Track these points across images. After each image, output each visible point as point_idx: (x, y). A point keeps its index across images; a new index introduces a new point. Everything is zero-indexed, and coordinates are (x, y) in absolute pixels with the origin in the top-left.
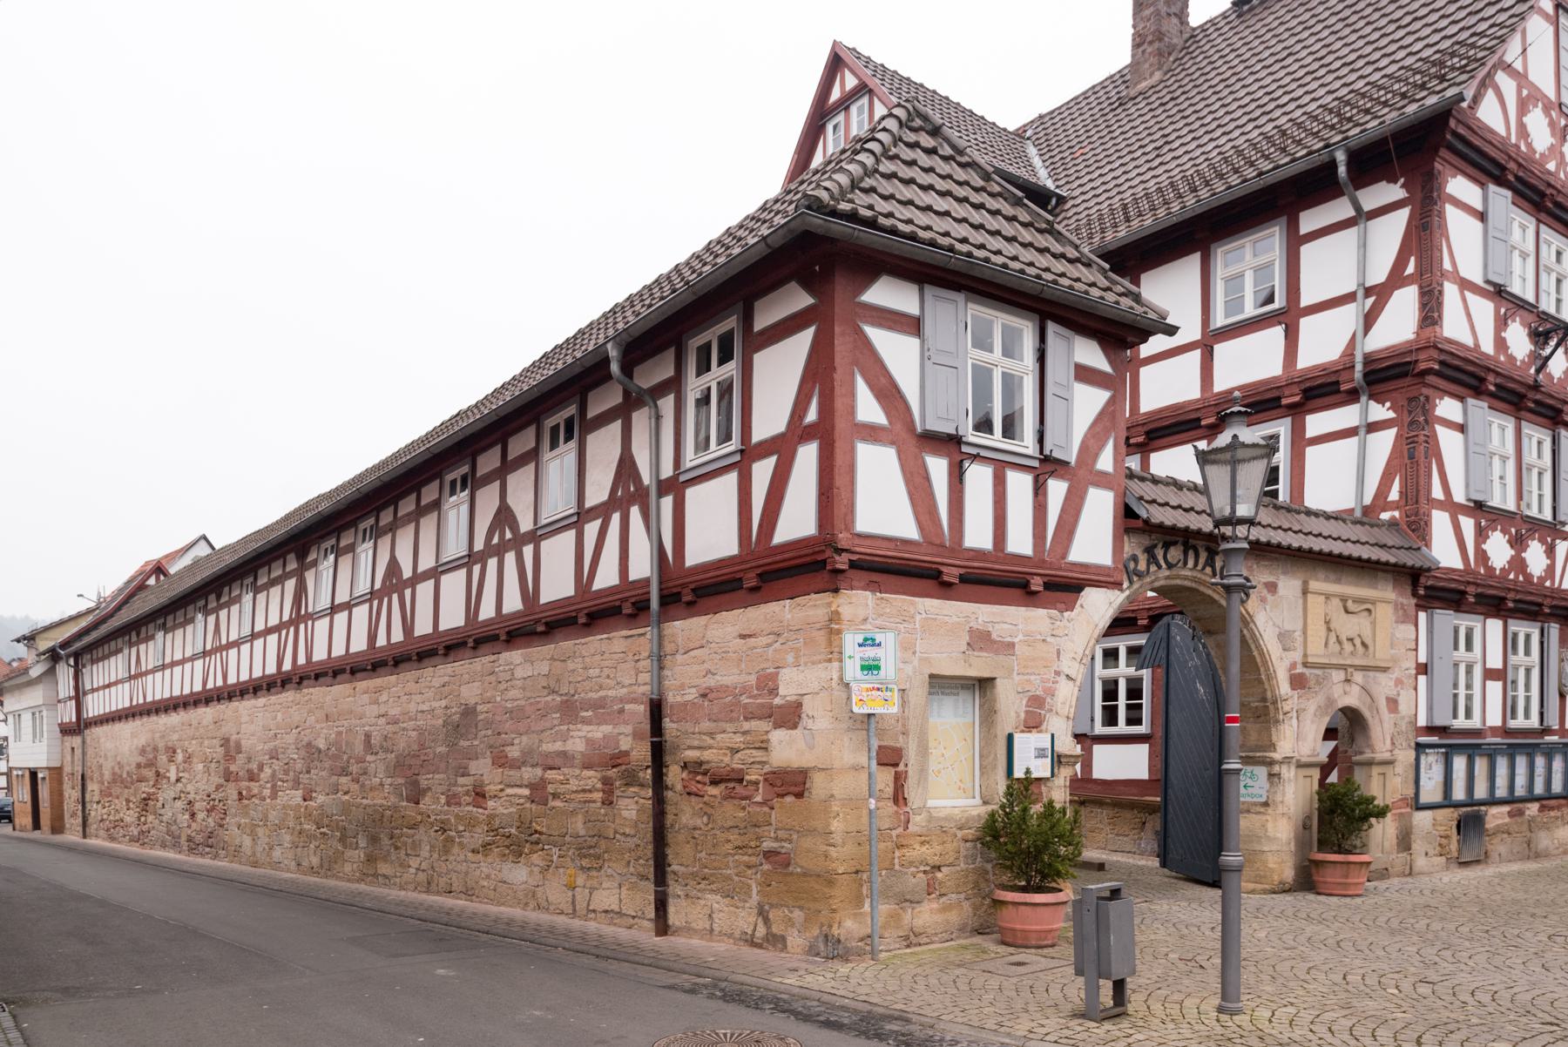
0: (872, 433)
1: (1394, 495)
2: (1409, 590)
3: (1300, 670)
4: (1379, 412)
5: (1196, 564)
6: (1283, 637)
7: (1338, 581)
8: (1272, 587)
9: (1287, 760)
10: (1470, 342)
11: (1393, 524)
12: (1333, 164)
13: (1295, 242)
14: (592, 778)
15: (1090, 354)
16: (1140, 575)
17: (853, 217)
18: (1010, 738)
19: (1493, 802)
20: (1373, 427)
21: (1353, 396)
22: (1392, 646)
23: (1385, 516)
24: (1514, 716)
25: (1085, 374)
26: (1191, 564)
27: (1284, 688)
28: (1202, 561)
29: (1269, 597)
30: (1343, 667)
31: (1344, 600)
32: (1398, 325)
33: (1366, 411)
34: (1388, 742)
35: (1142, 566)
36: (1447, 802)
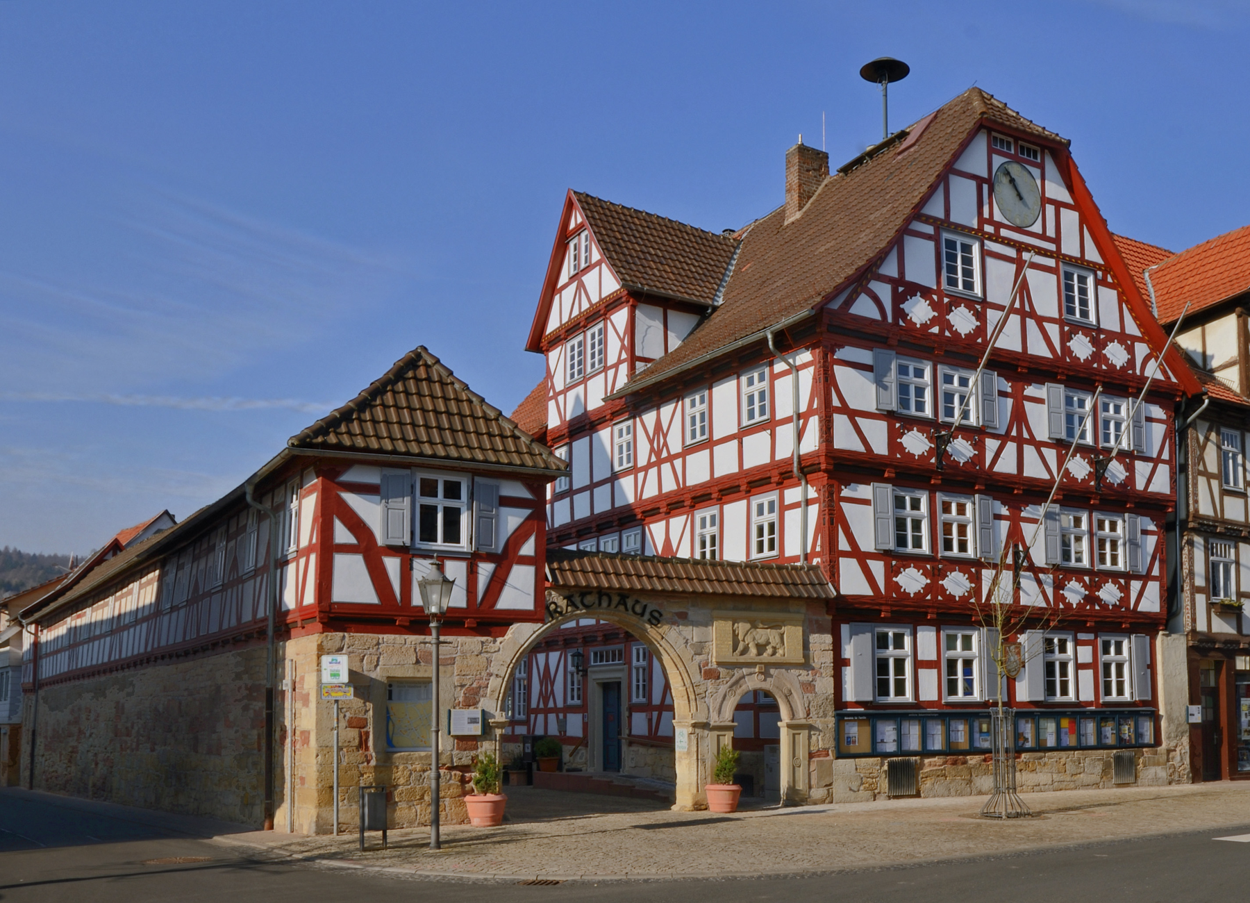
0: (346, 549)
1: (818, 549)
5: (609, 605)
10: (860, 448)
11: (817, 567)
13: (774, 377)
20: (808, 502)
23: (815, 561)
26: (605, 604)
28: (615, 602)
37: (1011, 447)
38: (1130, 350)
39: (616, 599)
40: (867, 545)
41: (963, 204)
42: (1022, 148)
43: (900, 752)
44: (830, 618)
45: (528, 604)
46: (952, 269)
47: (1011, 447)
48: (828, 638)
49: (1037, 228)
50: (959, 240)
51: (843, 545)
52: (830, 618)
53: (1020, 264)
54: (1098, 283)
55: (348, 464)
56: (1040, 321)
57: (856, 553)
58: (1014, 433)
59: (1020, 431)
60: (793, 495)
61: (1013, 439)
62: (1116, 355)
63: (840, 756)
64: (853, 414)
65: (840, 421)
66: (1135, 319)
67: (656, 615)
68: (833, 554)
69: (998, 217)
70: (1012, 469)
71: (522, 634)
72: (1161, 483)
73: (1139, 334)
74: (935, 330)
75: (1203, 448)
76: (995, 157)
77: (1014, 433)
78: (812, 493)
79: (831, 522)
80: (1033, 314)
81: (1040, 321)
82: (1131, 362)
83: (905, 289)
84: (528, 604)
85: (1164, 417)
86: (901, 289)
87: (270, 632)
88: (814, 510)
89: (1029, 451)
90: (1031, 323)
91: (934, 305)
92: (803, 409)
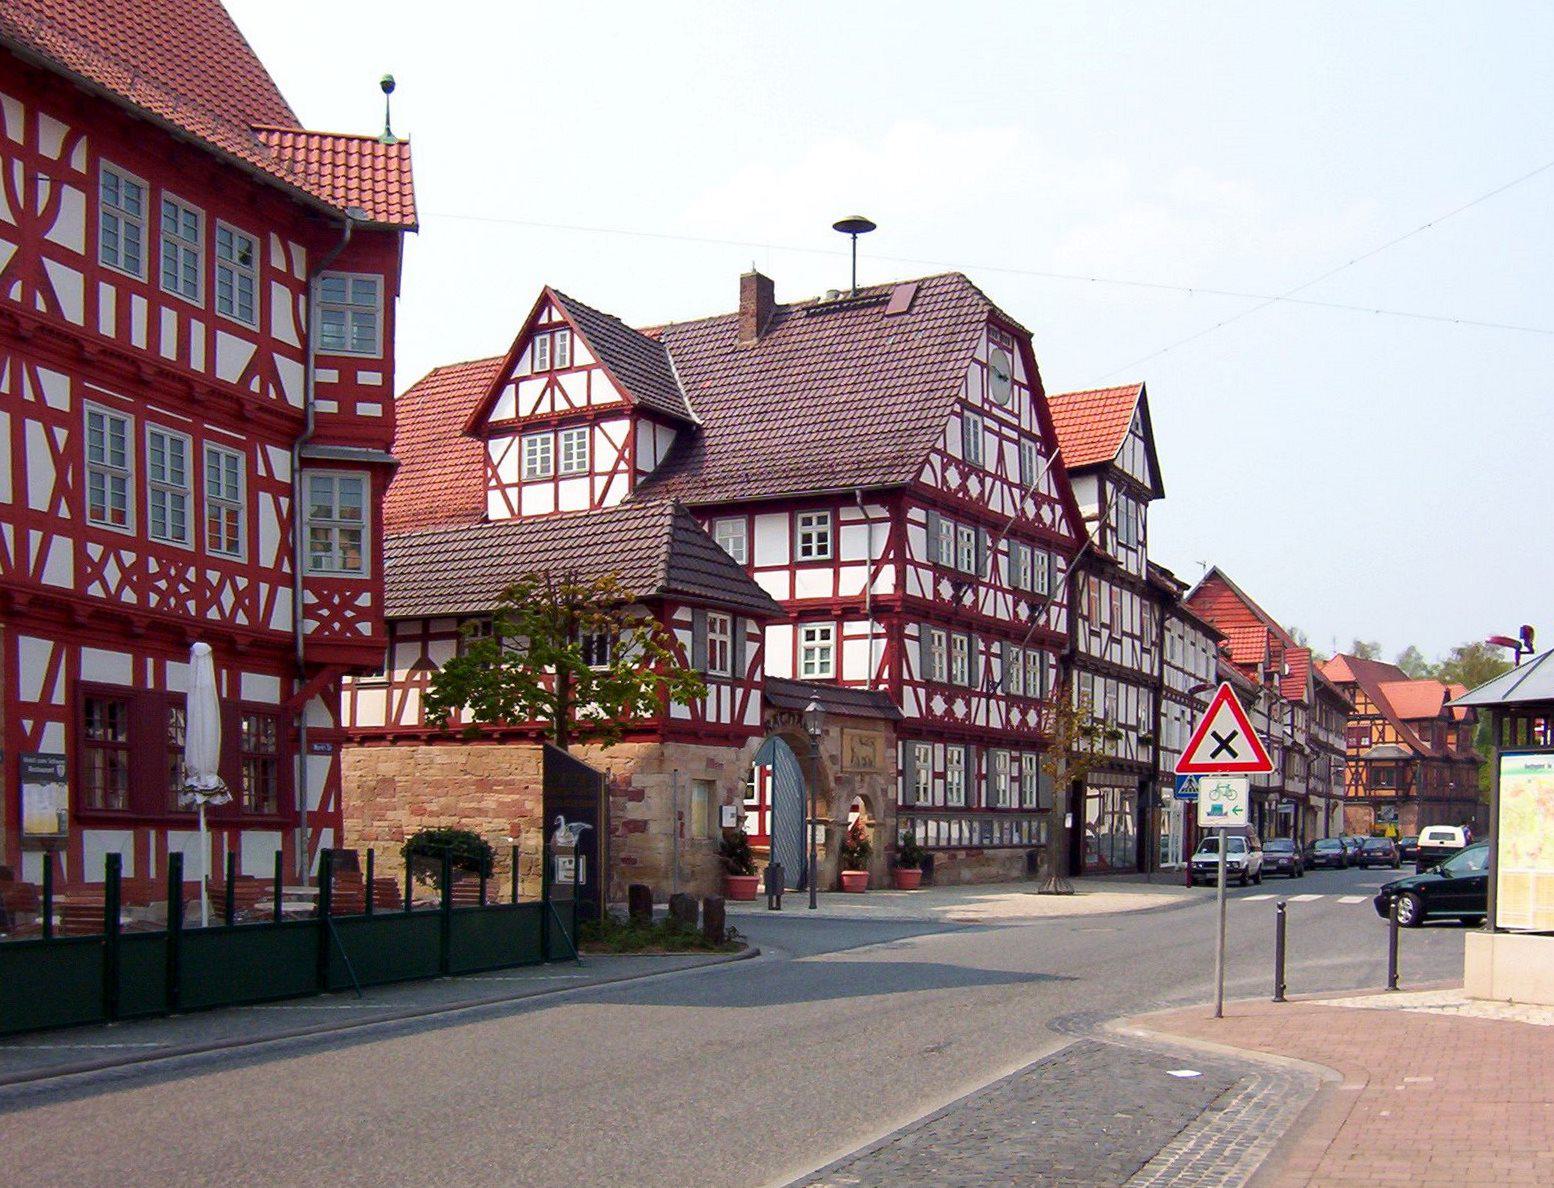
1: (886, 675)
4: (880, 629)
14: (503, 823)
20: (877, 636)
21: (865, 618)
23: (882, 687)
32: (886, 584)
44: (895, 735)
47: (991, 591)
49: (1008, 407)
52: (895, 735)
60: (852, 628)
69: (991, 398)
88: (883, 642)
92: (878, 556)
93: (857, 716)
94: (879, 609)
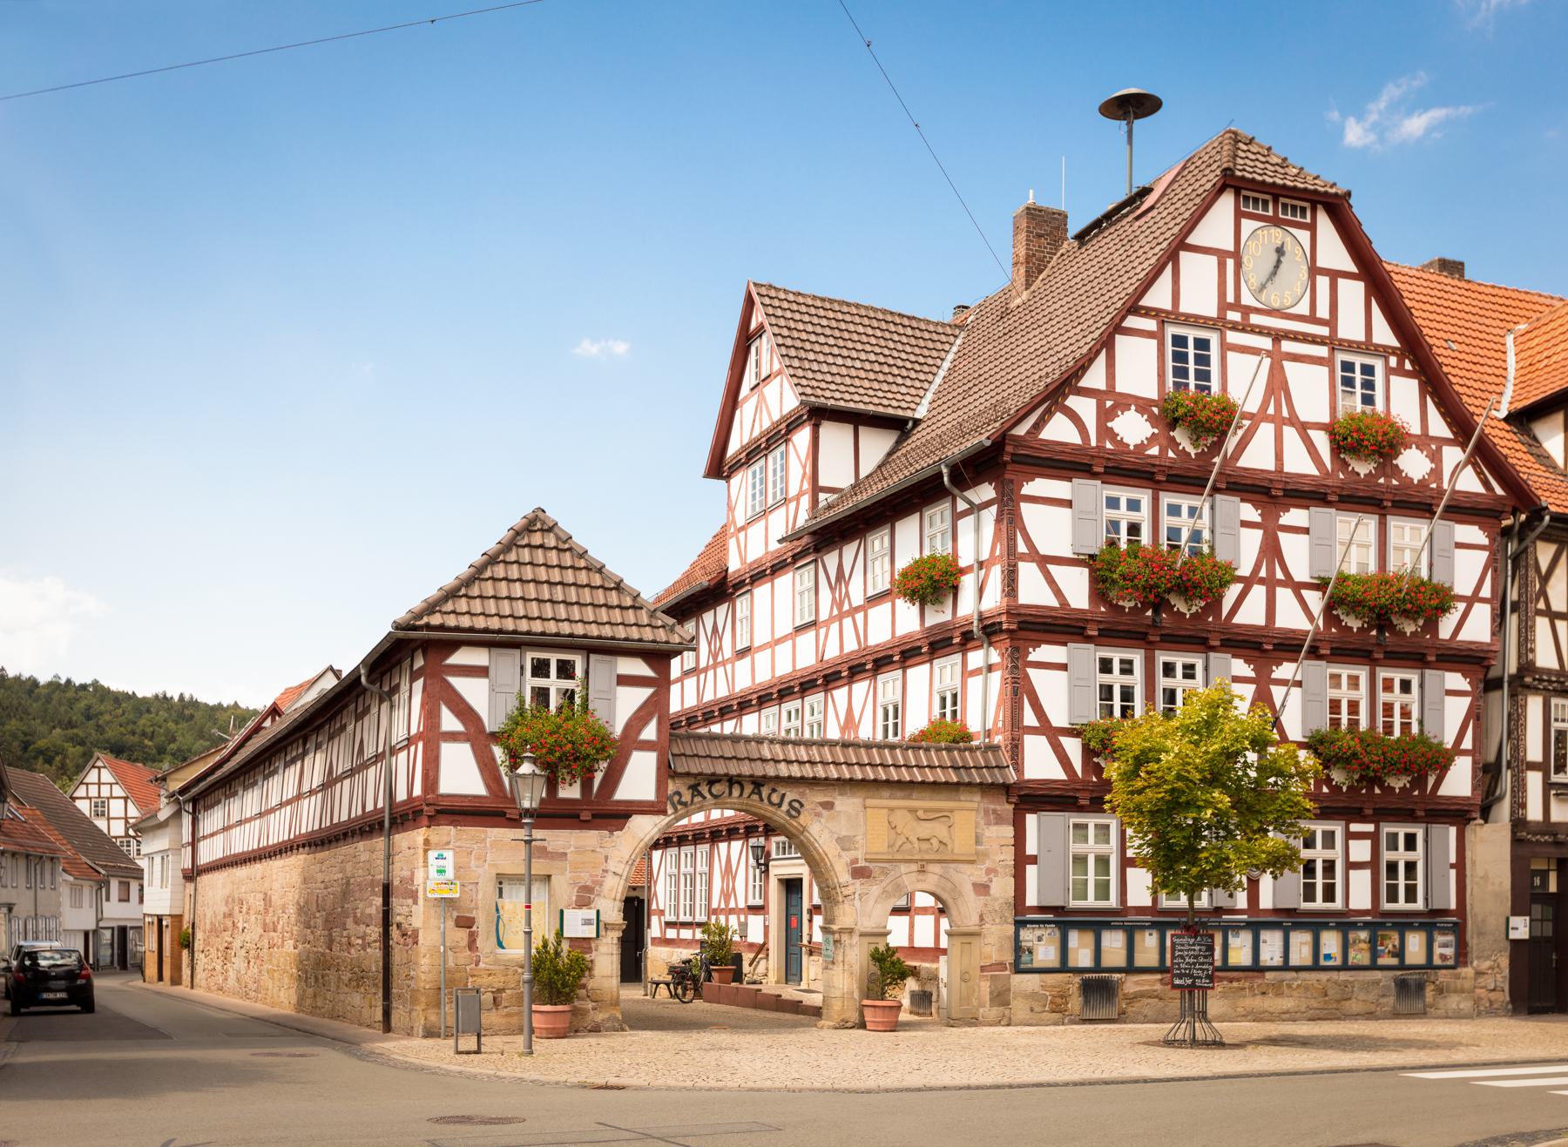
0: (453, 737)
2: (1004, 798)
3: (862, 864)
4: (995, 657)
6: (845, 843)
7: (909, 797)
8: (829, 806)
9: (851, 931)
10: (1054, 603)
12: (940, 474)
15: (639, 668)
16: (685, 804)
17: (428, 627)
18: (562, 912)
19: (1131, 969)
20: (990, 668)
22: (978, 841)
24: (1393, 897)
25: (624, 680)
26: (736, 793)
27: (843, 876)
28: (747, 791)
29: (825, 813)
30: (916, 861)
31: (913, 811)
33: (987, 655)
34: (975, 919)
35: (687, 797)
36: (1064, 967)
37: (1259, 592)
38: (1436, 457)
39: (748, 789)
40: (1059, 719)
41: (1198, 287)
42: (1285, 206)
43: (1097, 967)
45: (648, 793)
46: (1181, 372)
47: (1259, 592)
48: (1009, 831)
50: (1192, 334)
51: (1030, 719)
53: (1278, 360)
54: (1389, 371)
55: (454, 646)
56: (1303, 428)
57: (1046, 728)
58: (1263, 573)
59: (1271, 571)
60: (976, 658)
61: (1262, 581)
62: (1414, 464)
63: (1018, 971)
64: (1044, 561)
65: (1028, 573)
66: (1443, 415)
67: (796, 805)
68: (1017, 729)
70: (1260, 620)
71: (644, 827)
72: (1477, 628)
73: (1448, 434)
74: (1154, 451)
75: (1545, 579)
76: (1244, 221)
77: (1263, 573)
78: (995, 657)
79: (1015, 692)
80: (1293, 421)
81: (1303, 428)
82: (1436, 473)
83: (1112, 403)
84: (648, 793)
85: (1486, 541)
86: (1109, 404)
87: (387, 824)
88: (996, 678)
89: (1284, 596)
90: (1290, 433)
91: (1153, 420)
92: (985, 556)
93: (876, 782)
94: (990, 630)
